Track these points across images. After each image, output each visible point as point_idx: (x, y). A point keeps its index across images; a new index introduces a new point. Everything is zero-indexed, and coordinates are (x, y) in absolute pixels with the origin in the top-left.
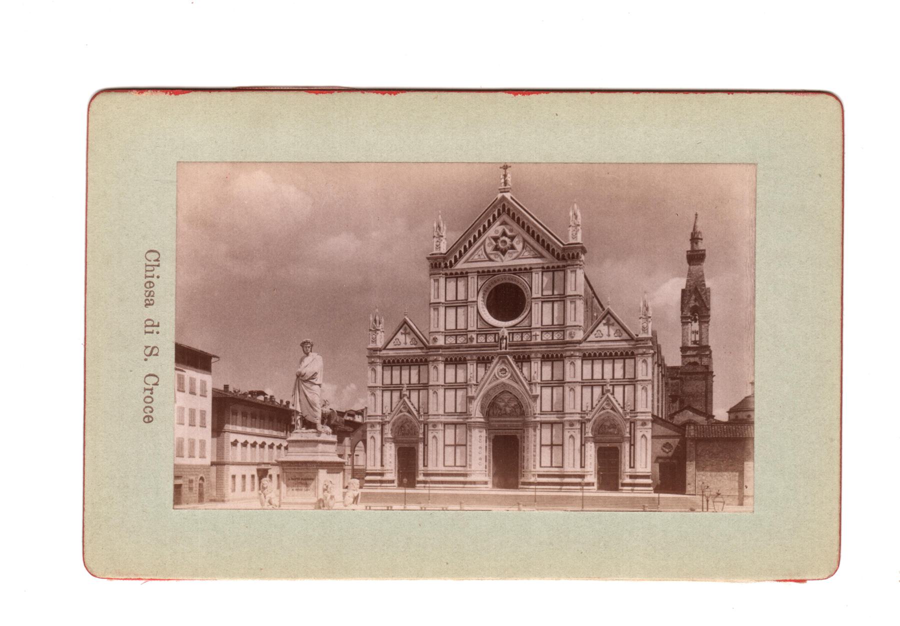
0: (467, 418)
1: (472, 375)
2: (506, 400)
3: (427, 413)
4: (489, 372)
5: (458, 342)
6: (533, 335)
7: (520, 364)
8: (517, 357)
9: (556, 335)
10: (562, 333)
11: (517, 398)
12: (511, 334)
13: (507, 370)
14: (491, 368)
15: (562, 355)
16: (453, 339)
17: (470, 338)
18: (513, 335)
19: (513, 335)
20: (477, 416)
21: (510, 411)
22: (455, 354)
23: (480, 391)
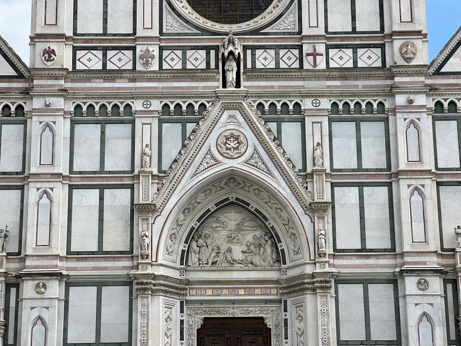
0: (137, 268)
1: (147, 150)
2: (232, 225)
3: (19, 253)
4: (191, 145)
5: (110, 66)
6: (308, 55)
7: (273, 126)
8: (267, 107)
9: (365, 58)
10: (378, 51)
11: (264, 217)
12: (249, 52)
13: (242, 139)
14: (200, 135)
15: (381, 103)
16: (95, 60)
17: (141, 57)
18: (253, 55)
19: (253, 55)
20: (160, 261)
21: (243, 252)
22: (103, 97)
23: (174, 189)
